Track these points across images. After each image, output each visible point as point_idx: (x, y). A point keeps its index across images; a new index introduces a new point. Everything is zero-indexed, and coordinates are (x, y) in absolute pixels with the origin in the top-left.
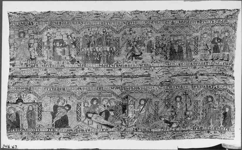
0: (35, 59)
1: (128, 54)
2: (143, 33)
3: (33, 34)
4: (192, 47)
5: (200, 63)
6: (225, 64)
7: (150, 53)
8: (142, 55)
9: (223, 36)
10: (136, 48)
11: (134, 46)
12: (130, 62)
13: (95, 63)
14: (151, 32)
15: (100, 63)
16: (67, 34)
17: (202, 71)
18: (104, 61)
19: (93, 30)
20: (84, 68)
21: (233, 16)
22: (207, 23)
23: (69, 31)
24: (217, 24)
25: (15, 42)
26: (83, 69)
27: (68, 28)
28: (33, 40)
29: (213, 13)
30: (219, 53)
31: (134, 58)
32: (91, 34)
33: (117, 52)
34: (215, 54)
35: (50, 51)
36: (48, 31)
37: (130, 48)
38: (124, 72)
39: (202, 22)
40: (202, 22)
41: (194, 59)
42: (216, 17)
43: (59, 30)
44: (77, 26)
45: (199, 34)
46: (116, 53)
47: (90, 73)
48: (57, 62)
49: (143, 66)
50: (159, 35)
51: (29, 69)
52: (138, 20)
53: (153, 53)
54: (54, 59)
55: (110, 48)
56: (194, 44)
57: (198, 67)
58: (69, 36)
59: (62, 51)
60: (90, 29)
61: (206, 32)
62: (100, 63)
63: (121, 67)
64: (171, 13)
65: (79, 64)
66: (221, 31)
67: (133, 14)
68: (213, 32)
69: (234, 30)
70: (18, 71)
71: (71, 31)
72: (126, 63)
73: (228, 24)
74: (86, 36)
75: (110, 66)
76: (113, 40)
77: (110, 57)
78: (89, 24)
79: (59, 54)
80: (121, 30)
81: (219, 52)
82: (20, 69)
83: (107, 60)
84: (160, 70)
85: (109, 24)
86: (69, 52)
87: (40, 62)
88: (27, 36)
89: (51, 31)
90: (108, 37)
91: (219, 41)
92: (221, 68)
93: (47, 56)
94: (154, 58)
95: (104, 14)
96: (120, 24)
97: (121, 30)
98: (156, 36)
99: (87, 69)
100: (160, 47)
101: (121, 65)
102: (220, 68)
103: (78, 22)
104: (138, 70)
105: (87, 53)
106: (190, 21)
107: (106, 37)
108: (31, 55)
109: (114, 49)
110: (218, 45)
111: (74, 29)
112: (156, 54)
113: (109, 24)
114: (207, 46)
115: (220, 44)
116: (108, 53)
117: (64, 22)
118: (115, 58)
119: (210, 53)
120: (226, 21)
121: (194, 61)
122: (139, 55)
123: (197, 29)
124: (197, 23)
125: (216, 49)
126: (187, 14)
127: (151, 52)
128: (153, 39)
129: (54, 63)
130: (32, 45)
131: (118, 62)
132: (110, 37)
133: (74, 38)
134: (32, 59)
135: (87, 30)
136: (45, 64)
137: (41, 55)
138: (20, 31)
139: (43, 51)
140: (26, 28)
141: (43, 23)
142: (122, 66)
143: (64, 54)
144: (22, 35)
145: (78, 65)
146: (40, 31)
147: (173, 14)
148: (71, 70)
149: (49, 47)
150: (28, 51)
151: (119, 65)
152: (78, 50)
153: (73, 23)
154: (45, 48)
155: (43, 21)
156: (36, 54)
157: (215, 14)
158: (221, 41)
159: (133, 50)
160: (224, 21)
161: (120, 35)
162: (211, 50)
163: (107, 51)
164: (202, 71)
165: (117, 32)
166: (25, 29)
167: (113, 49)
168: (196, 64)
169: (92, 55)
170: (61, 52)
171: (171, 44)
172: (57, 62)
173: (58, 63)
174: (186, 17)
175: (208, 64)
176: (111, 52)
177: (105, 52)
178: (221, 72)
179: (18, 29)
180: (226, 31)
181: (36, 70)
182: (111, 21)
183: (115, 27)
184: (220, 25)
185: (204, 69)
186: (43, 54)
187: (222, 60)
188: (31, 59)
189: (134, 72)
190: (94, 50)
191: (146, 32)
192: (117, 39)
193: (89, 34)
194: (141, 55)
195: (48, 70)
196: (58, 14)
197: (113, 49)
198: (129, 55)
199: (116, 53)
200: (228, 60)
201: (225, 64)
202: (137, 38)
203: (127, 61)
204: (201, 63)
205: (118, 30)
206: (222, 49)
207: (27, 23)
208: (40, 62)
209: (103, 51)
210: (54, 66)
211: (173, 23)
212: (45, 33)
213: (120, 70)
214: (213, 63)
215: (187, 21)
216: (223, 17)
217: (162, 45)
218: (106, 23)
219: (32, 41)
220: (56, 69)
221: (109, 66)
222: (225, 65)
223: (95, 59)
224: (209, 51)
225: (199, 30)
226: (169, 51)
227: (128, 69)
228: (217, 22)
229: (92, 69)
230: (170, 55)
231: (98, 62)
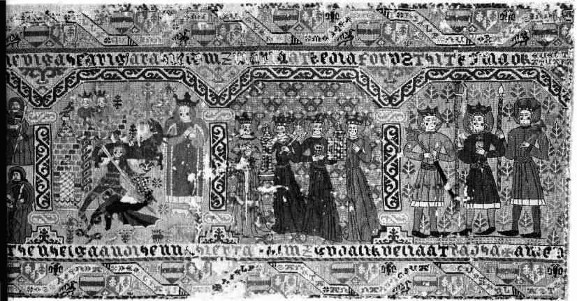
1: (88, 201)
5: (411, 248)
6: (525, 251)
8: (154, 205)
9: (509, 125)
10: (123, 174)
12: (97, 236)
14: (187, 100)
22: (436, 64)
24: (483, 71)
31: (115, 216)
33: (40, 189)
34: (480, 206)
37: (98, 173)
39: (414, 61)
41: (384, 229)
42: (475, 38)
45: (399, 116)
46: (37, 194)
49: (158, 253)
50: (227, 116)
52: (132, 46)
56: (380, 158)
57: (400, 267)
63: (60, 257)
66: (501, 102)
73: (529, 71)
81: (497, 200)
84: (232, 277)
91: (492, 148)
96: (53, 65)
101: (58, 247)
102: (503, 271)
106: (357, 54)
109: (30, 177)
115: (499, 163)
120: (523, 59)
121: (385, 236)
122: (138, 206)
123: (391, 92)
124: (389, 64)
125: (482, 188)
126: (343, 19)
131: (44, 235)
142: (62, 254)
151: (48, 247)
158: (500, 148)
167: (23, 178)
171: (278, 158)
174: (338, 34)
175: (449, 253)
184: (495, 75)
187: (513, 233)
189: (117, 279)
192: (40, 132)
194: (145, 204)
199: (37, 194)
201: (525, 251)
204: (415, 248)
205: (42, 93)
206: (506, 184)
213: (56, 269)
216: (503, 41)
227: (92, 266)
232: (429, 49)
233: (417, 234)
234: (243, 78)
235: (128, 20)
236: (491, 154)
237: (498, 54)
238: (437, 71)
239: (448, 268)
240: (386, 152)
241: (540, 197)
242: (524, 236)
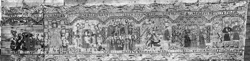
0: (66, 47)
1: (147, 42)
2: (161, 23)
3: (65, 25)
4: (205, 36)
5: (212, 50)
6: (235, 50)
7: (167, 41)
9: (233, 25)
10: (154, 36)
11: (153, 34)
12: (149, 49)
13: (119, 50)
15: (123, 50)
16: (94, 24)
17: (214, 57)
18: (126, 48)
19: (116, 21)
20: (110, 54)
21: (242, 8)
22: (218, 14)
23: (96, 22)
25: (49, 32)
26: (108, 55)
27: (95, 19)
28: (65, 30)
29: (223, 5)
31: (153, 45)
32: (115, 24)
34: (226, 41)
35: (79, 39)
36: (78, 22)
37: (149, 36)
38: (144, 57)
39: (214, 13)
40: (214, 13)
42: (227, 9)
43: (87, 21)
44: (103, 18)
45: (210, 24)
47: (114, 58)
48: (85, 49)
49: (161, 52)
50: (175, 24)
51: (61, 55)
52: (157, 11)
53: (169, 41)
54: (83, 47)
55: (132, 37)
56: (206, 33)
57: (210, 53)
58: (96, 27)
59: (90, 39)
60: (114, 20)
62: (123, 50)
63: (142, 53)
64: (186, 6)
65: (105, 51)
66: (231, 21)
67: (152, 7)
68: (224, 22)
70: (51, 57)
71: (98, 22)
72: (145, 50)
74: (111, 26)
75: (132, 52)
76: (135, 29)
77: (132, 44)
78: (113, 16)
79: (88, 42)
80: (141, 21)
81: (229, 40)
82: (54, 55)
83: (129, 47)
84: (176, 56)
85: (130, 15)
86: (96, 41)
87: (71, 49)
88: (59, 27)
89: (80, 22)
90: (130, 27)
91: (229, 30)
92: (232, 54)
93: (77, 44)
94: (171, 45)
95: (126, 6)
96: (141, 15)
97: (141, 21)
98: (172, 25)
99: (112, 55)
100: (176, 35)
102: (230, 54)
103: (103, 14)
104: (157, 55)
105: (112, 41)
107: (128, 26)
108: (63, 43)
109: (136, 37)
110: (228, 34)
111: (100, 21)
112: (173, 42)
113: (130, 15)
114: (218, 35)
115: (231, 33)
116: (130, 41)
117: (91, 14)
118: (137, 45)
119: (221, 40)
120: (237, 12)
121: (207, 48)
122: (157, 43)
123: (209, 19)
125: (227, 38)
127: (168, 40)
128: (169, 28)
129: (83, 50)
130: (63, 34)
132: (132, 26)
133: (101, 28)
134: (64, 47)
135: (112, 21)
136: (75, 51)
137: (71, 43)
138: (53, 22)
139: (74, 40)
140: (58, 19)
141: (74, 15)
142: (142, 52)
143: (92, 42)
144: (55, 25)
145: (104, 52)
146: (70, 22)
147: (187, 7)
148: (98, 56)
149: (78, 36)
150: (60, 39)
151: (139, 51)
152: (104, 39)
153: (100, 15)
154: (75, 37)
155: (73, 13)
156: (67, 42)
157: (225, 6)
158: (231, 30)
159: (152, 37)
160: (234, 12)
161: (140, 25)
162: (222, 38)
163: (129, 39)
164: (214, 57)
165: (138, 23)
166: (57, 20)
167: (134, 38)
169: (116, 43)
170: (89, 40)
171: (186, 33)
172: (85, 49)
173: (87, 50)
174: (199, 9)
175: (220, 51)
176: (133, 40)
177: (127, 40)
178: (232, 58)
179: (51, 20)
181: (67, 56)
182: (133, 12)
183: (136, 17)
184: (231, 16)
186: (73, 42)
188: (63, 46)
190: (118, 38)
191: (164, 22)
193: (114, 24)
194: (159, 42)
195: (78, 56)
196: (86, 8)
197: (134, 38)
198: (149, 43)
200: (238, 47)
201: (235, 50)
202: (155, 28)
203: (147, 47)
204: (213, 50)
205: (138, 21)
206: (232, 37)
207: (59, 15)
208: (71, 49)
209: (126, 39)
210: (83, 52)
211: (187, 14)
212: (75, 24)
213: (141, 55)
214: (224, 50)
215: (200, 13)
216: (233, 9)
217: (178, 34)
218: (128, 14)
219: (64, 31)
220: (85, 55)
221: (131, 52)
223: (119, 46)
224: (220, 39)
226: (184, 39)
228: (227, 14)
229: (116, 55)
230: (185, 42)
231: (122, 49)
232: (217, 11)
233: (213, 47)
234: (179, 17)
235: (156, 6)
236: (229, 31)
237: (231, 12)
238: (219, 15)
239: (220, 54)
240: (207, 31)
241: (239, 40)
242: (235, 47)
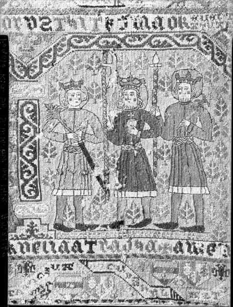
6: (185, 247)
9: (166, 100)
30: (154, 193)
57: (40, 265)
61: (77, 79)
66: (156, 73)
68: (114, 79)
69: (221, 68)
81: (153, 187)
91: (147, 127)
92: (168, 270)
110: (142, 152)
115: (155, 144)
158: (156, 127)
168: (35, 250)
180: (182, 74)
184: (149, 42)
185: (77, 275)
204: (58, 243)
206: (164, 169)
222: (186, 253)
225: (42, 66)
228: (131, 28)
